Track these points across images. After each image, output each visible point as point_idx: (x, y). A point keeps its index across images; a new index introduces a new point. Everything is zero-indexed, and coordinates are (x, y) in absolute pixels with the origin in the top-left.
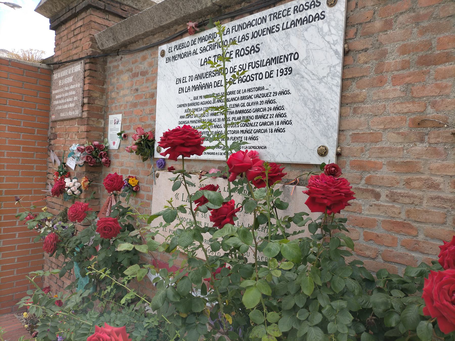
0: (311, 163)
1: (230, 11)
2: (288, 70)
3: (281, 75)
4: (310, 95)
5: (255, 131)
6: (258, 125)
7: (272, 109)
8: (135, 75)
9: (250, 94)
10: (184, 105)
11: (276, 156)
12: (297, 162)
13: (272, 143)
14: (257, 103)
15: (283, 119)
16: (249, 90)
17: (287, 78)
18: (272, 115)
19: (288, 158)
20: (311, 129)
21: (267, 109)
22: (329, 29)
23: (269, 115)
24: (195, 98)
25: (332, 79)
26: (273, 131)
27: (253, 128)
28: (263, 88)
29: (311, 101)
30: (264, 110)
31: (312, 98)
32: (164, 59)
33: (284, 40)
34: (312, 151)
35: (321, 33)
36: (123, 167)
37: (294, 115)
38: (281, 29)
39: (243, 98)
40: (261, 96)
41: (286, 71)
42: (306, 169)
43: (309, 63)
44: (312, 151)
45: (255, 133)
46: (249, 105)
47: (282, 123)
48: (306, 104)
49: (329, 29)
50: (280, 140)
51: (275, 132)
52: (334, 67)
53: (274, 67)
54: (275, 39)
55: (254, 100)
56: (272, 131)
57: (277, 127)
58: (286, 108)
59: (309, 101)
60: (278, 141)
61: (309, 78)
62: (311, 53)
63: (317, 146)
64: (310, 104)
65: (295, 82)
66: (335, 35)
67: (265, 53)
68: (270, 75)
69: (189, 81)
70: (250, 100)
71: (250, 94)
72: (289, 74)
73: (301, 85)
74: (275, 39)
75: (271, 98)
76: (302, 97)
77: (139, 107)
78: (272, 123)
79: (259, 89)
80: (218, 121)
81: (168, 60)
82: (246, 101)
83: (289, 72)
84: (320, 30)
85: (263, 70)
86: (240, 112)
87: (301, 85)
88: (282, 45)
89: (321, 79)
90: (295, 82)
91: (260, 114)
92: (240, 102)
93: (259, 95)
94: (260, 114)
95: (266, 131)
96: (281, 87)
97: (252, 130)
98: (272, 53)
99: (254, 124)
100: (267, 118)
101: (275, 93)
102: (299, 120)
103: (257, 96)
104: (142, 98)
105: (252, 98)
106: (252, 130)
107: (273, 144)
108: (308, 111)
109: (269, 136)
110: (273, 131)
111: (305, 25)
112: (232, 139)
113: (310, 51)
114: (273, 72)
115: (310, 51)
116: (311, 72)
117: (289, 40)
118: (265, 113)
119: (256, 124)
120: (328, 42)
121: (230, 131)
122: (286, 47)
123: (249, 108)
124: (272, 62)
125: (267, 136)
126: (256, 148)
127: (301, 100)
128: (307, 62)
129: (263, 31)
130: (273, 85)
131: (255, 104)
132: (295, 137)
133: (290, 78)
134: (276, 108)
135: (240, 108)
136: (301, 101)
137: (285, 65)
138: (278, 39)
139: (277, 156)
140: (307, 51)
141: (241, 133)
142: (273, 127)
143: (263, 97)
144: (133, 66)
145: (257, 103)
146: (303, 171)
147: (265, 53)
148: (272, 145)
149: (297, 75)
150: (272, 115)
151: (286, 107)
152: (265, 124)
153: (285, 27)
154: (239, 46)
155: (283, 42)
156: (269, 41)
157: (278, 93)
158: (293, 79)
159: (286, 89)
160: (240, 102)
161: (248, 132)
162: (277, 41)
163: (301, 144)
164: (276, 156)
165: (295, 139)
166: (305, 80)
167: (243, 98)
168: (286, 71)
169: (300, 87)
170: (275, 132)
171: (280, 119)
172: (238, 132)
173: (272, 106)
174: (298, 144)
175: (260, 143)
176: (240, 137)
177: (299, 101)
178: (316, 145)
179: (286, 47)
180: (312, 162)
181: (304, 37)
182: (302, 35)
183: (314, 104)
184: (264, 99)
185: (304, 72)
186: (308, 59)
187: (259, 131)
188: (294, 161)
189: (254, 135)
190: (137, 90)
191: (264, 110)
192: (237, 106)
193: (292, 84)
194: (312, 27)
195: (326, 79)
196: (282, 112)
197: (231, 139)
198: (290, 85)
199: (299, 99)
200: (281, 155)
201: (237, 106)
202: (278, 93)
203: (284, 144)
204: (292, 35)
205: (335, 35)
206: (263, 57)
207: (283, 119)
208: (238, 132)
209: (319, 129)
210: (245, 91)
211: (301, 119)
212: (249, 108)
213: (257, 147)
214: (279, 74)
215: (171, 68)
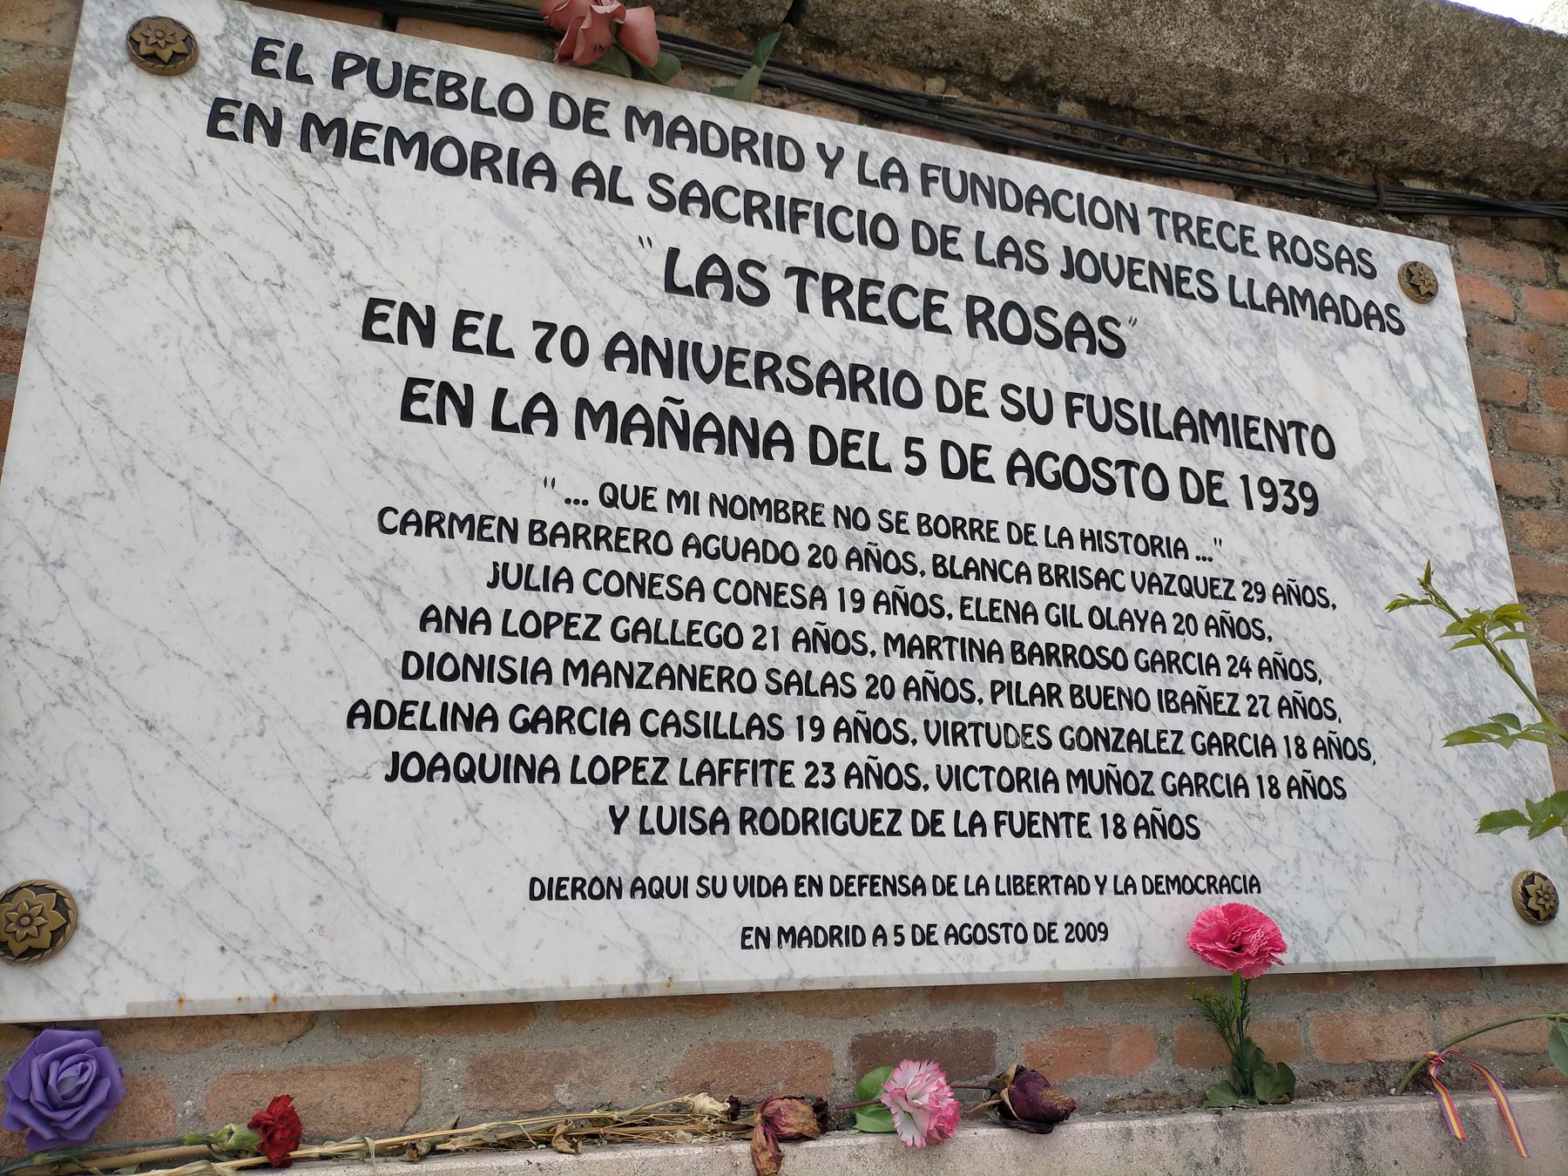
0: (1498, 963)
1: (867, 79)
2: (1295, 492)
3: (1268, 508)
4: (1422, 629)
5: (1170, 781)
6: (1184, 744)
7: (1254, 666)
9: (1106, 561)
10: (476, 527)
11: (1323, 932)
12: (1437, 961)
13: (1291, 862)
14: (1158, 621)
15: (1321, 728)
16: (1092, 539)
17: (1299, 528)
18: (1261, 703)
19: (1386, 938)
20: (1463, 792)
21: (1225, 666)
22: (1432, 380)
23: (1242, 700)
24: (613, 496)
25: (1491, 581)
26: (1283, 787)
27: (1157, 764)
28: (1179, 549)
29: (1433, 659)
30: (1209, 665)
31: (1432, 647)
33: (1250, 350)
34: (1490, 898)
35: (1403, 383)
37: (1372, 714)
38: (1224, 296)
39: (1054, 576)
40: (1174, 587)
41: (1288, 493)
42: (1451, 995)
43: (1384, 490)
44: (1490, 898)
45: (1172, 794)
46: (1105, 623)
47: (1326, 748)
48: (1413, 671)
49: (1432, 380)
50: (1332, 841)
51: (1295, 793)
52: (1485, 533)
53: (1216, 454)
54: (1204, 332)
55: (1131, 600)
56: (1274, 786)
57: (1297, 768)
58: (1329, 672)
59: (1425, 659)
60: (1320, 847)
61: (1402, 557)
62: (1382, 448)
63: (1506, 874)
64: (1433, 674)
65: (1342, 559)
66: (1455, 409)
67: (1156, 374)
68: (1208, 490)
69: (541, 354)
70: (1107, 598)
71: (1106, 561)
72: (1308, 513)
73: (1374, 579)
74: (1204, 332)
75: (1238, 609)
76: (1391, 634)
78: (1265, 746)
79: (1153, 546)
80: (869, 695)
82: (1084, 600)
83: (1303, 505)
84: (1398, 373)
85: (1170, 455)
86: (1049, 655)
87: (1374, 579)
88: (1245, 370)
89: (1450, 571)
90: (1342, 559)
91: (1183, 683)
92: (1036, 594)
93: (1165, 581)
94: (1183, 683)
95: (1237, 786)
96: (1282, 565)
97: (1150, 774)
98: (1199, 388)
99: (1160, 741)
100: (1231, 713)
101: (1255, 591)
102: (1400, 742)
103: (1151, 583)
105: (1122, 589)
106: (1150, 774)
107: (1297, 861)
108: (1432, 705)
109: (1263, 819)
110: (1283, 787)
111: (1330, 329)
112: (1005, 829)
113: (1377, 439)
114: (1223, 480)
115: (1377, 439)
116: (1404, 532)
117: (1273, 361)
118: (1213, 683)
119: (1171, 739)
120: (1441, 431)
121: (988, 769)
122: (1265, 384)
123: (1109, 639)
124: (1208, 429)
125: (1249, 815)
126: (1195, 887)
127: (1389, 646)
128: (1375, 481)
129: (1130, 268)
130: (1235, 544)
131: (1143, 622)
132: (1401, 827)
133: (1314, 530)
134: (1276, 668)
135: (1042, 634)
136: (1390, 653)
137: (1279, 464)
138: (1218, 335)
139: (1330, 930)
140: (1366, 435)
141: (1078, 790)
142: (1282, 768)
143: (1188, 594)
145: (1158, 621)
146: (1437, 1007)
147: (1156, 374)
148: (1293, 872)
149: (1345, 528)
150: (1261, 703)
151: (1323, 665)
152: (1226, 744)
153: (1241, 294)
154: (997, 286)
155: (1248, 357)
156: (1171, 328)
157: (1269, 592)
158: (1329, 539)
159: (1308, 578)
160: (1036, 594)
161: (1121, 786)
162: (1213, 343)
163: (1435, 865)
164: (1323, 932)
165: (1403, 838)
166: (1385, 557)
167: (1054, 576)
168: (1288, 493)
169: (1372, 588)
170: (1295, 793)
171: (1312, 730)
172: (1048, 781)
173: (1254, 651)
174: (1419, 862)
175: (1219, 859)
176: (1068, 815)
177: (1382, 649)
178: (1500, 870)
179: (1265, 384)
180: (1504, 958)
181: (1337, 370)
182: (1329, 363)
183: (1448, 675)
184: (1201, 608)
185: (1373, 521)
186: (1378, 470)
187: (1198, 784)
188: (1423, 955)
189: (1170, 806)
191: (1209, 665)
192: (1022, 613)
193: (1332, 565)
194: (1361, 344)
195: (1466, 573)
196: (1309, 690)
197: (998, 824)
198: (1321, 561)
199: (1380, 643)
200: (1347, 923)
201: (1022, 613)
202: (1269, 592)
203: (1353, 863)
204: (1286, 347)
205: (1455, 409)
206: (1152, 390)
207: (1321, 728)
208: (1048, 781)
209: (1495, 795)
210: (1065, 537)
211: (1408, 739)
212: (1109, 639)
213: (1202, 884)
214: (1259, 501)
215: (297, 200)
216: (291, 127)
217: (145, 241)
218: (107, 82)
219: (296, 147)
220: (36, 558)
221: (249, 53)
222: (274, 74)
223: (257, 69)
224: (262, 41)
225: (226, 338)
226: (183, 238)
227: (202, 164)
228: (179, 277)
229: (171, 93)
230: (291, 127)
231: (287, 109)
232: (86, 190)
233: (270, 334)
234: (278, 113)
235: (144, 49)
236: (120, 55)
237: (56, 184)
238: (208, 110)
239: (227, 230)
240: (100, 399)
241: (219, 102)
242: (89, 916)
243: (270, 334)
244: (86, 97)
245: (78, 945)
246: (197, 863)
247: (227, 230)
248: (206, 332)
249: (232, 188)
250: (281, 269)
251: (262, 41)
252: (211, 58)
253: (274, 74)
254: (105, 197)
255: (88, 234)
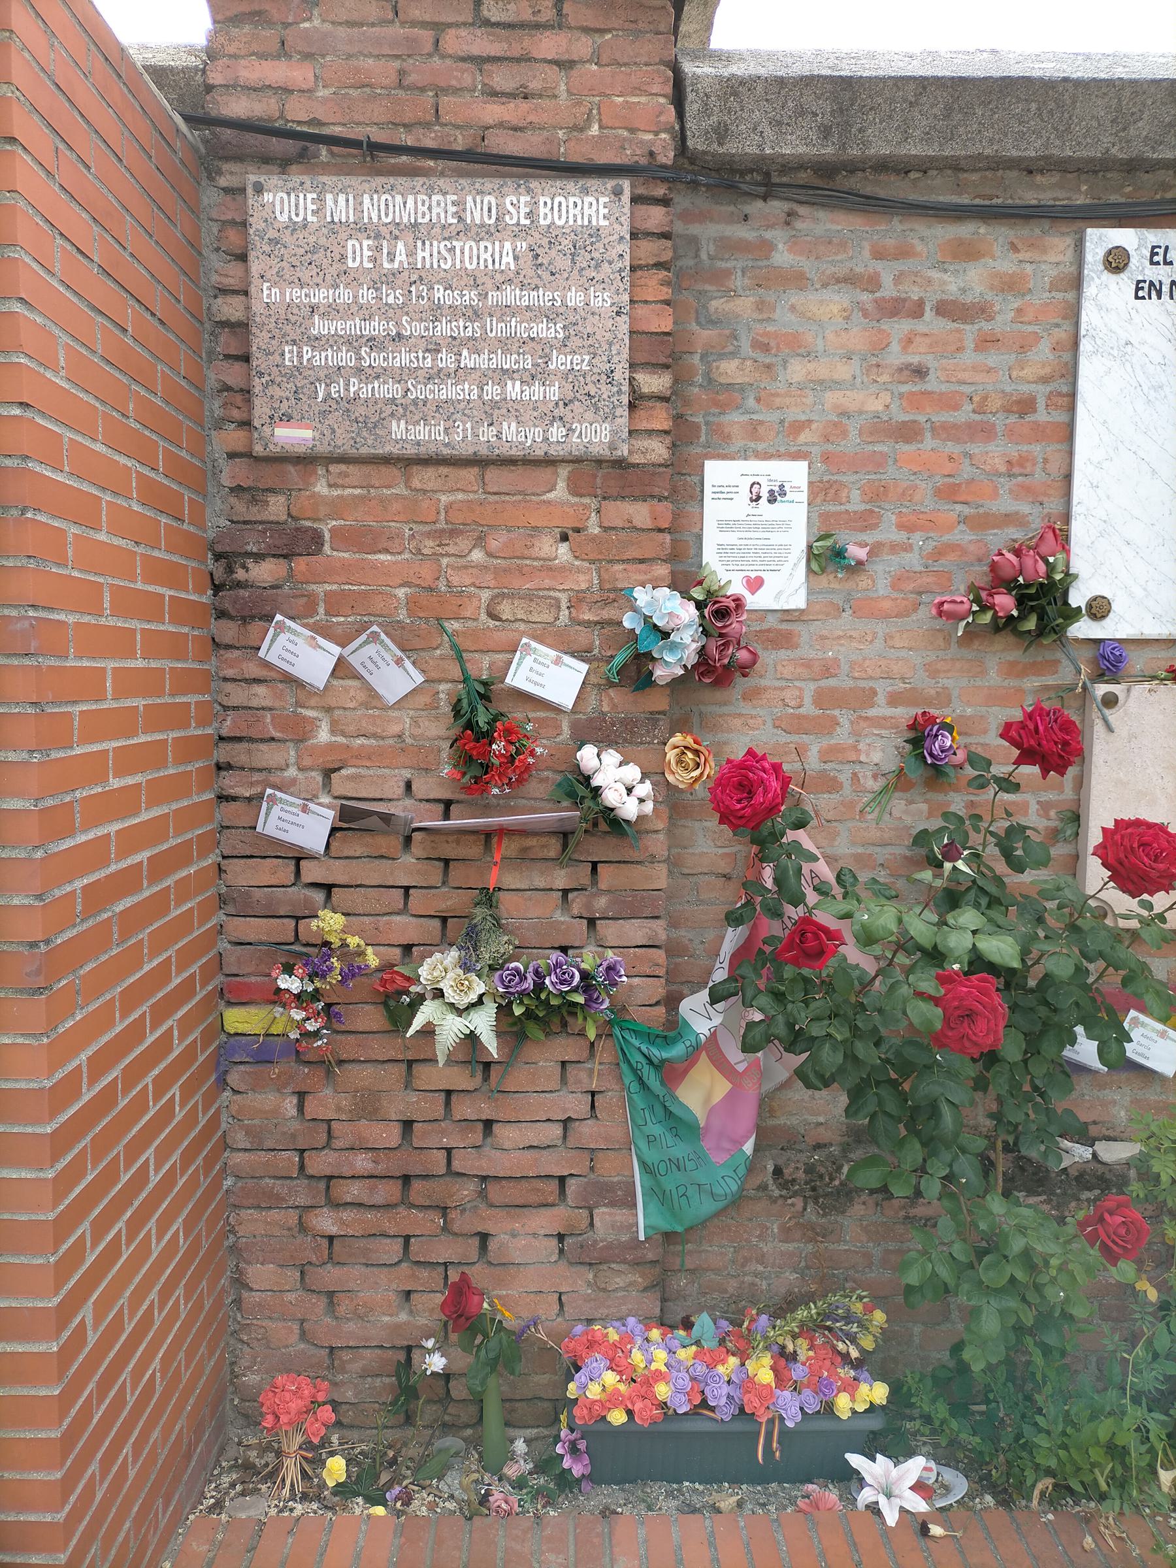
8: (895, 308)
32: (1123, 284)
36: (832, 682)
77: (929, 442)
81: (1146, 290)
104: (956, 407)
144: (887, 272)
190: (920, 372)
216: (1166, 289)
217: (1115, 352)
218: (1097, 281)
219: (1168, 297)
220: (1089, 485)
221: (1148, 255)
222: (1158, 263)
223: (1152, 263)
224: (1154, 247)
225: (1146, 391)
226: (1129, 348)
227: (1133, 313)
228: (1128, 365)
229: (1120, 282)
230: (1166, 289)
231: (1164, 281)
232: (1094, 333)
233: (1161, 387)
234: (1161, 283)
235: (1114, 265)
236: (1102, 267)
237: (1083, 332)
238: (1134, 287)
239: (1143, 343)
240: (1105, 422)
241: (1139, 282)
242: (1114, 606)
243: (1161, 387)
244: (1090, 290)
245: (1111, 615)
246: (1145, 590)
247: (1143, 343)
248: (1139, 389)
249: (1145, 323)
250: (1164, 358)
251: (1154, 247)
252: (1134, 261)
253: (1158, 263)
254: (1101, 335)
255: (1096, 352)
